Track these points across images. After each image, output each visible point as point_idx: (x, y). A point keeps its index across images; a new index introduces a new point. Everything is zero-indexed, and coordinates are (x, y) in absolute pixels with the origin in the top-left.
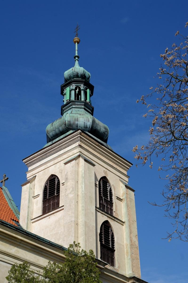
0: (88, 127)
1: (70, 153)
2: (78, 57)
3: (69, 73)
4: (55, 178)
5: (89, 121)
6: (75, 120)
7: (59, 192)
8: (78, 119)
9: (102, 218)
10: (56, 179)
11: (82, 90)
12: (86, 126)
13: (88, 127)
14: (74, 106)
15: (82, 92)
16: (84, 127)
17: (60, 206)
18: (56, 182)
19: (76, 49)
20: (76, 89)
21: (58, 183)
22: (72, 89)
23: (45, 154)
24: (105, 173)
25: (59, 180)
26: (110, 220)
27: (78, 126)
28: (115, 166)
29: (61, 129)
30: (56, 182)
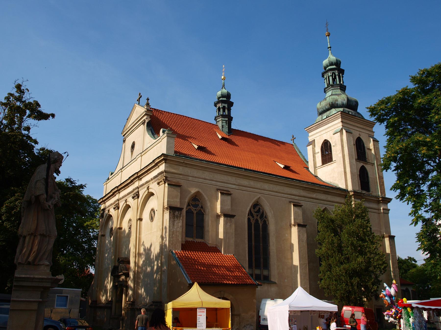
0: (345, 104)
1: (336, 126)
2: (330, 47)
3: (326, 63)
4: (328, 142)
5: (344, 100)
6: (335, 100)
8: (337, 100)
9: (361, 164)
10: (328, 142)
11: (337, 75)
12: (343, 103)
13: (345, 104)
14: (333, 88)
15: (337, 77)
16: (342, 105)
17: (333, 160)
18: (329, 145)
19: (328, 41)
20: (333, 74)
21: (330, 145)
23: (319, 125)
24: (359, 135)
25: (330, 143)
26: (364, 165)
27: (338, 104)
28: (365, 127)
29: (327, 107)
30: (329, 145)
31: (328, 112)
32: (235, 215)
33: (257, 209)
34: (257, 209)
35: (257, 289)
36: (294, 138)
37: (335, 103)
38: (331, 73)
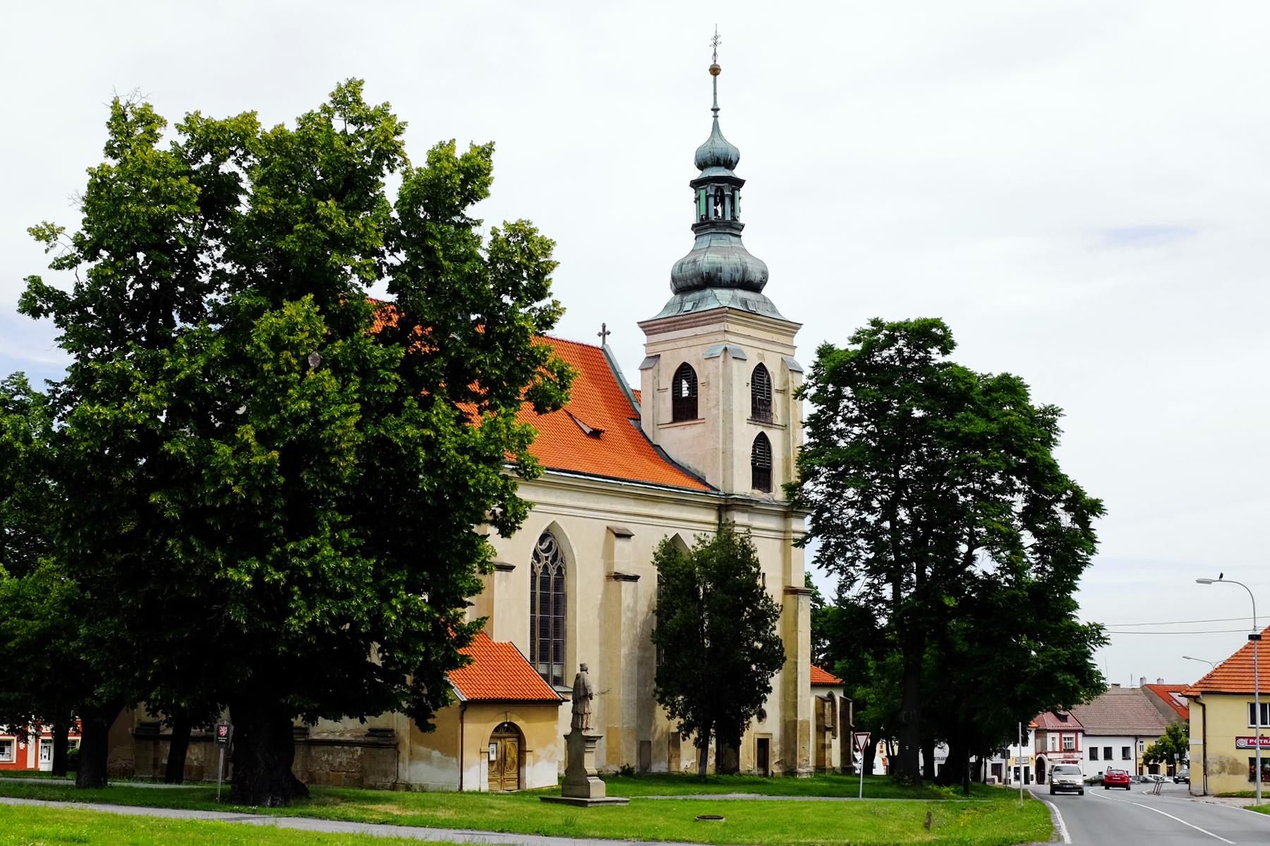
1: (712, 338)
7: (697, 394)
9: (759, 429)
14: (714, 230)
17: (699, 417)
28: (776, 338)
29: (695, 281)
31: (697, 295)
32: (514, 567)
33: (544, 547)
34: (548, 544)
35: (560, 707)
36: (604, 333)
38: (714, 189)
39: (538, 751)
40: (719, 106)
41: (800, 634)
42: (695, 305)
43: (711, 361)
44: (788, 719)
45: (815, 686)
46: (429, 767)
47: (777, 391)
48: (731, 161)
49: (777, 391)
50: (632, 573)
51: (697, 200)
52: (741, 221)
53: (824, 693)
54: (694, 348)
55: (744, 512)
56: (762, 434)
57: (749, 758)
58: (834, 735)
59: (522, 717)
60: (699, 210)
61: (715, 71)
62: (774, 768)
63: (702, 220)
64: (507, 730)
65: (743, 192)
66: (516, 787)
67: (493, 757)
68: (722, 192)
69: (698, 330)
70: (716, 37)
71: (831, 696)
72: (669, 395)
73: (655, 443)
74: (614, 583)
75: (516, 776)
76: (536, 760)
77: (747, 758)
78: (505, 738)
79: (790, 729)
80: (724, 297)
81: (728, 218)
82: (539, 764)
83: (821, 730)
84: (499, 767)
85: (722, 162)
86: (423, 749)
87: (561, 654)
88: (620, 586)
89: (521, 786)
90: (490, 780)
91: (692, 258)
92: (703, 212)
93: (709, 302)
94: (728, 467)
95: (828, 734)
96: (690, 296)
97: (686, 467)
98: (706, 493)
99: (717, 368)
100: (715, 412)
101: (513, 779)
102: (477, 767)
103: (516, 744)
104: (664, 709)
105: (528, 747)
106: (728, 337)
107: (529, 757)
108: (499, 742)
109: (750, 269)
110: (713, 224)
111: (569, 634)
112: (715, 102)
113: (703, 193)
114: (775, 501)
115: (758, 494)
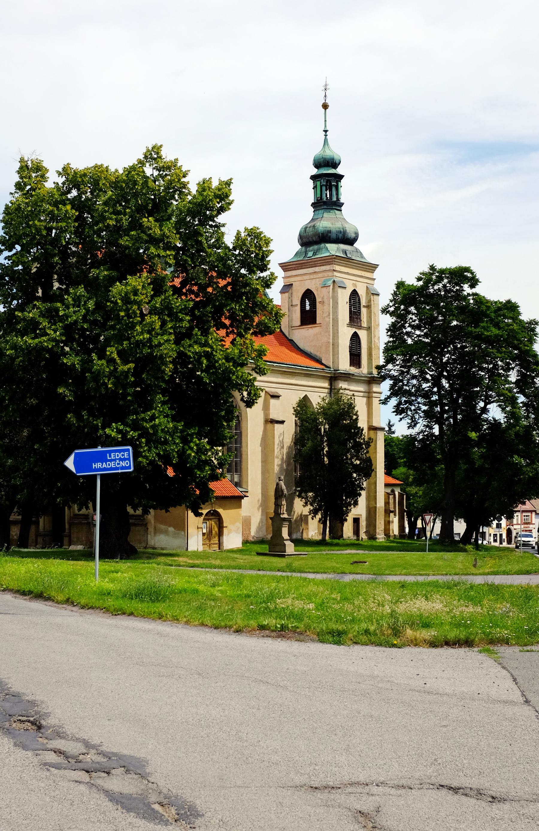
1: (325, 274)
6: (328, 231)
7: (316, 308)
9: (354, 330)
14: (325, 207)
17: (317, 322)
20: (327, 182)
22: (323, 185)
29: (314, 239)
31: (316, 247)
35: (242, 500)
37: (327, 235)
38: (325, 181)
39: (230, 527)
40: (327, 128)
41: (378, 455)
42: (315, 254)
43: (325, 288)
44: (371, 506)
45: (387, 485)
46: (167, 537)
47: (364, 306)
48: (336, 163)
49: (364, 306)
50: (280, 419)
51: (315, 188)
52: (342, 201)
53: (389, 490)
54: (314, 280)
55: (345, 381)
56: (355, 333)
57: (349, 529)
58: (395, 515)
59: (221, 507)
60: (316, 194)
61: (325, 106)
62: (363, 535)
63: (317, 200)
64: (212, 515)
65: (343, 182)
66: (218, 548)
67: (205, 531)
68: (331, 183)
69: (317, 269)
70: (326, 85)
71: (393, 491)
72: (298, 309)
73: (290, 338)
74: (270, 425)
75: (217, 542)
76: (229, 533)
77: (348, 529)
78: (211, 519)
79: (371, 512)
80: (333, 249)
81: (334, 199)
82: (231, 535)
83: (388, 512)
84: (208, 536)
85: (330, 164)
86: (163, 527)
87: (239, 468)
88: (274, 427)
89: (221, 547)
90: (203, 544)
91: (312, 224)
92: (319, 195)
93: (323, 252)
94: (336, 353)
95: (392, 515)
96: (311, 248)
97: (309, 353)
98: (323, 369)
99: (329, 292)
100: (327, 319)
101: (216, 544)
102: (196, 537)
103: (218, 523)
104: (301, 501)
105: (225, 525)
106: (336, 274)
107: (225, 531)
108: (208, 522)
109: (348, 231)
110: (325, 203)
111: (244, 456)
112: (325, 126)
113: (318, 183)
114: (363, 374)
115: (353, 370)
